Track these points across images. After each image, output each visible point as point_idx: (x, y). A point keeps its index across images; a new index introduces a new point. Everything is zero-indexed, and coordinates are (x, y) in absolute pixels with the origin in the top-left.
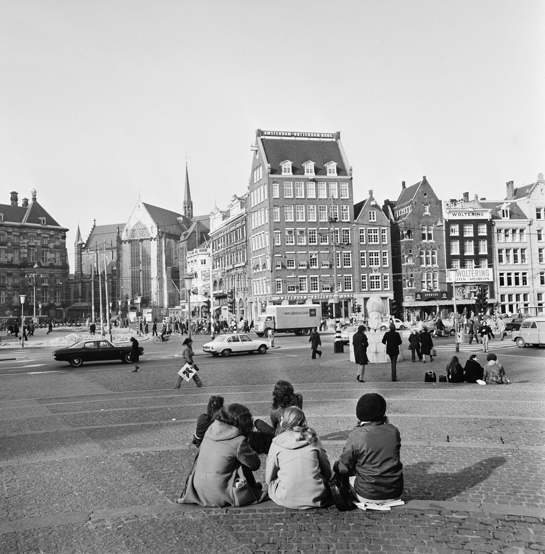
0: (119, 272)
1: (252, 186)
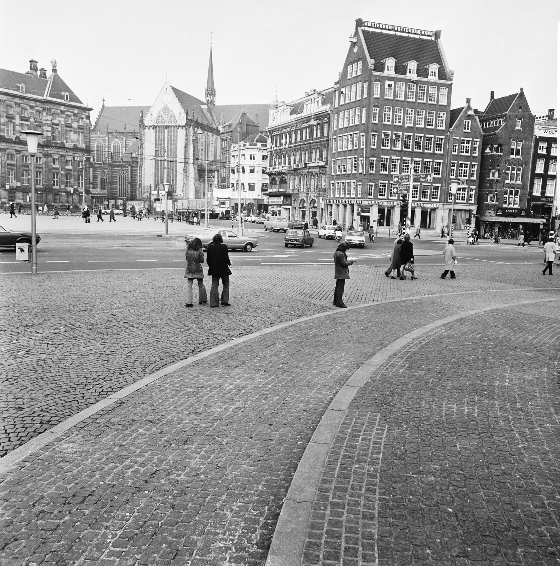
0: (141, 159)
1: (343, 81)
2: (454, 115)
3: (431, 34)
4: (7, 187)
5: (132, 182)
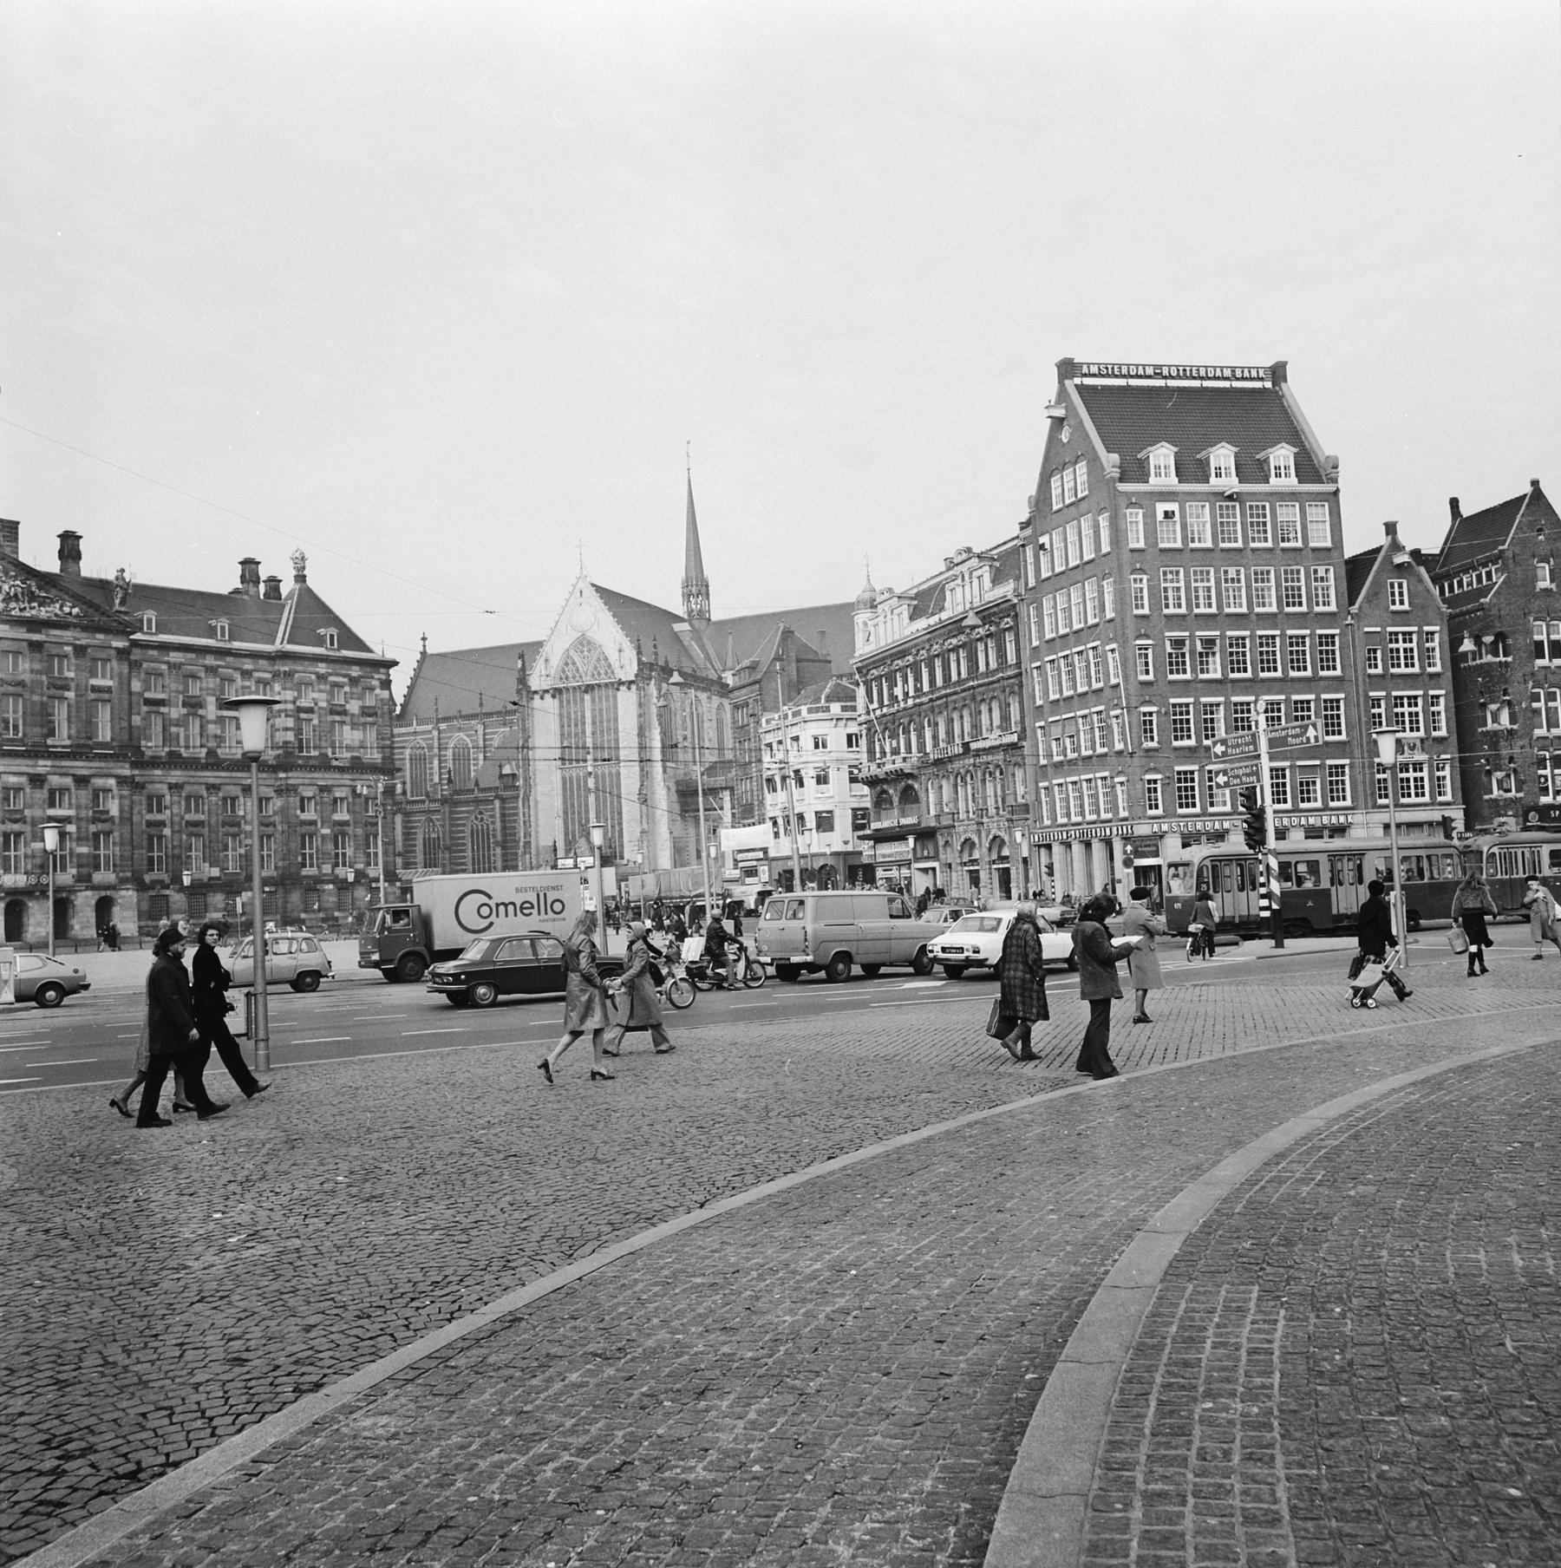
2: (1357, 568)
3: (1261, 374)
4: (187, 881)
5: (505, 841)
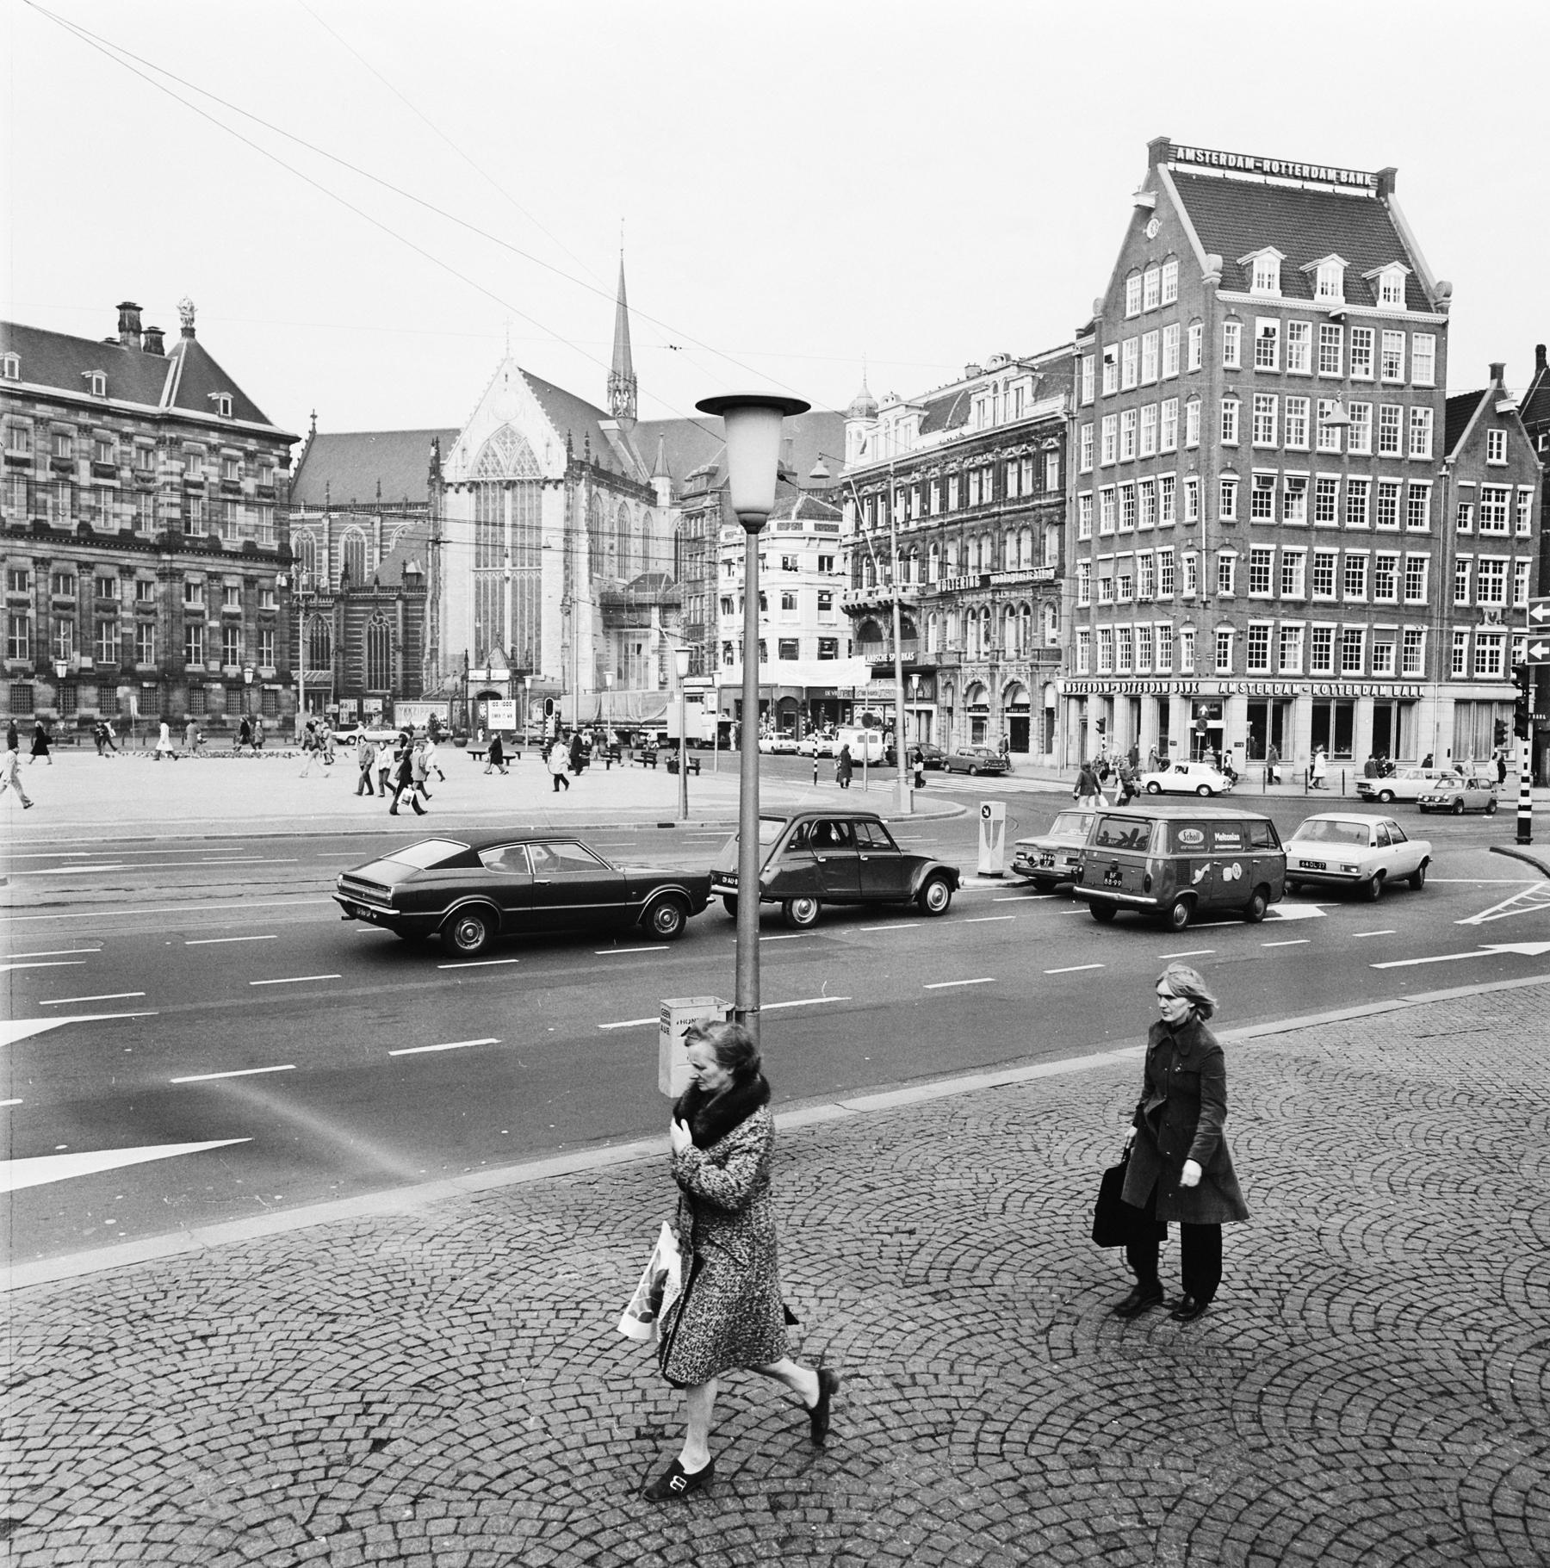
2: (1459, 410)
3: (1368, 182)
4: (61, 672)
5: (406, 646)
